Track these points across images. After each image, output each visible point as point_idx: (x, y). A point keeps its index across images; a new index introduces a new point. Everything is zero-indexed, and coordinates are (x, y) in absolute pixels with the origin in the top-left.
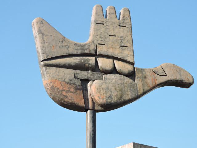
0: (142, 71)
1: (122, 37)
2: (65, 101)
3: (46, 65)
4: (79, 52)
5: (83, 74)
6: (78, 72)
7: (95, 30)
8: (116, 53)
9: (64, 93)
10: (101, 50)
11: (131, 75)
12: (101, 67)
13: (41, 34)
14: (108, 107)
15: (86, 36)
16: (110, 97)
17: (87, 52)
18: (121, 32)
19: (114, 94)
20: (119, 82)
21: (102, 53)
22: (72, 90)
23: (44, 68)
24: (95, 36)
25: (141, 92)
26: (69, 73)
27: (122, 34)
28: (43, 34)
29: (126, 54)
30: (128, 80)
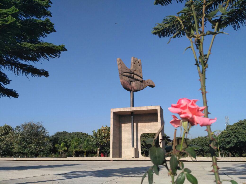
0: (144, 81)
1: (140, 69)
2: (126, 87)
3: (122, 75)
4: (130, 72)
5: (131, 80)
6: (130, 78)
7: (134, 65)
8: (138, 74)
9: (127, 85)
10: (135, 72)
11: (142, 82)
12: (135, 78)
13: (120, 64)
14: (136, 91)
15: (131, 67)
16: (138, 88)
17: (132, 72)
18: (139, 67)
19: (139, 87)
20: (140, 84)
21: (135, 73)
22: (129, 84)
23: (121, 76)
24: (133, 67)
25: (144, 88)
26: (127, 79)
27: (140, 68)
28: (121, 64)
29: (140, 75)
30: (141, 83)
